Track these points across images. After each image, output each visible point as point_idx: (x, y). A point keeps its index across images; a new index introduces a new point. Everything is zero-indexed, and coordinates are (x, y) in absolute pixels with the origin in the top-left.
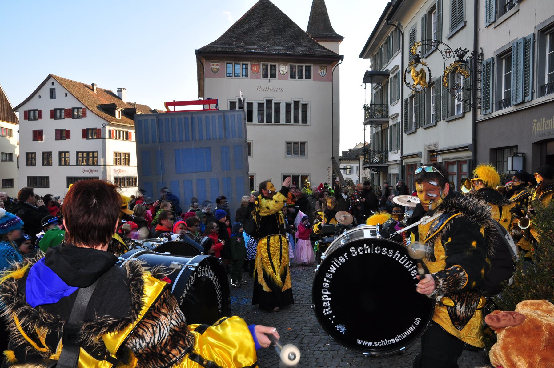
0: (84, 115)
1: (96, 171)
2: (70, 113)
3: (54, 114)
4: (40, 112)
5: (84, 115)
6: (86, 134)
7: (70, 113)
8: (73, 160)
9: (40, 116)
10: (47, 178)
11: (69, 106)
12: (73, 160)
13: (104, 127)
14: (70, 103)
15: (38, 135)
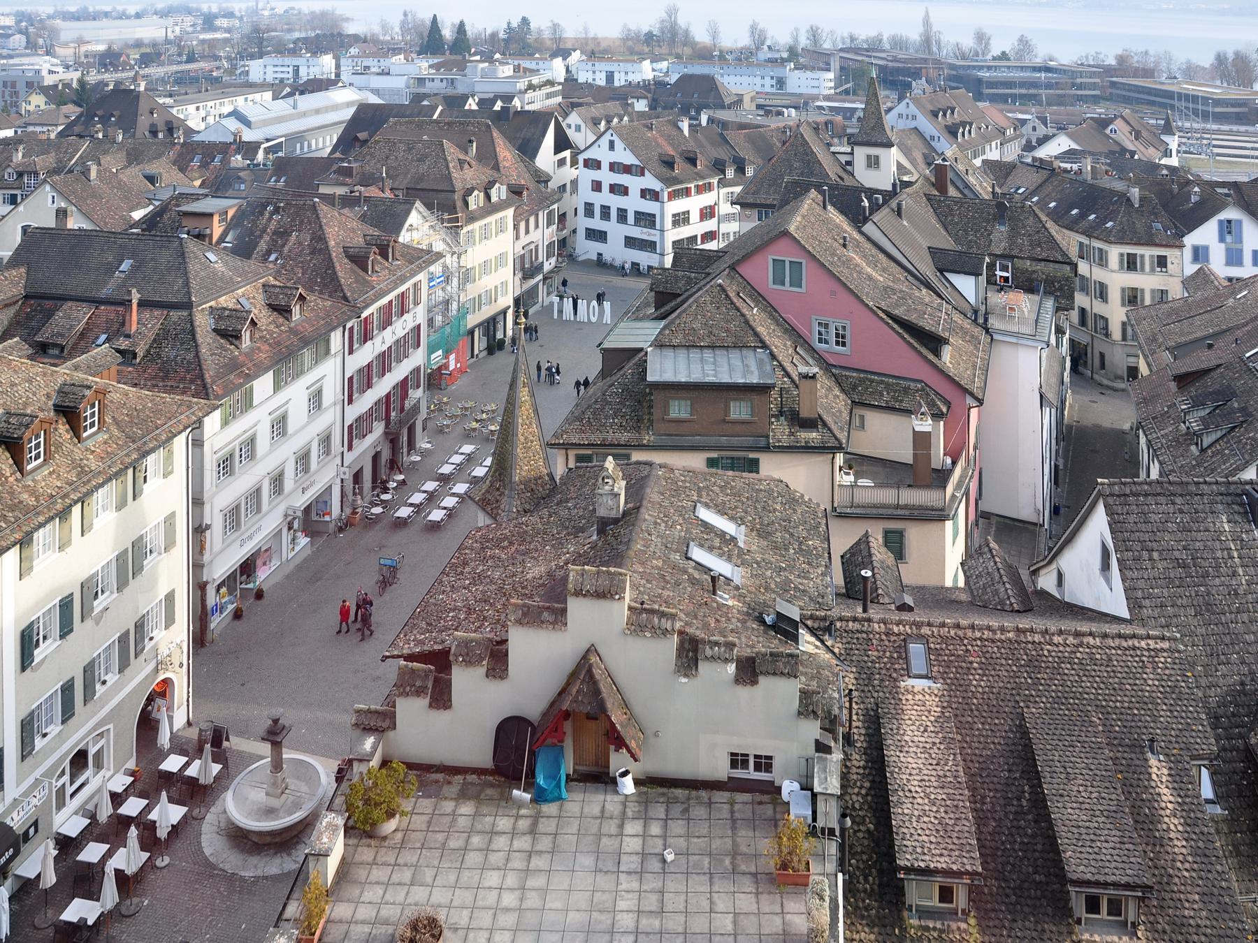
0: (643, 174)
1: (655, 235)
2: (627, 169)
3: (613, 167)
4: (599, 163)
5: (643, 174)
6: (645, 193)
7: (627, 169)
8: (631, 218)
9: (599, 168)
10: (606, 233)
11: (627, 162)
12: (631, 218)
13: (662, 190)
14: (629, 158)
15: (597, 186)
